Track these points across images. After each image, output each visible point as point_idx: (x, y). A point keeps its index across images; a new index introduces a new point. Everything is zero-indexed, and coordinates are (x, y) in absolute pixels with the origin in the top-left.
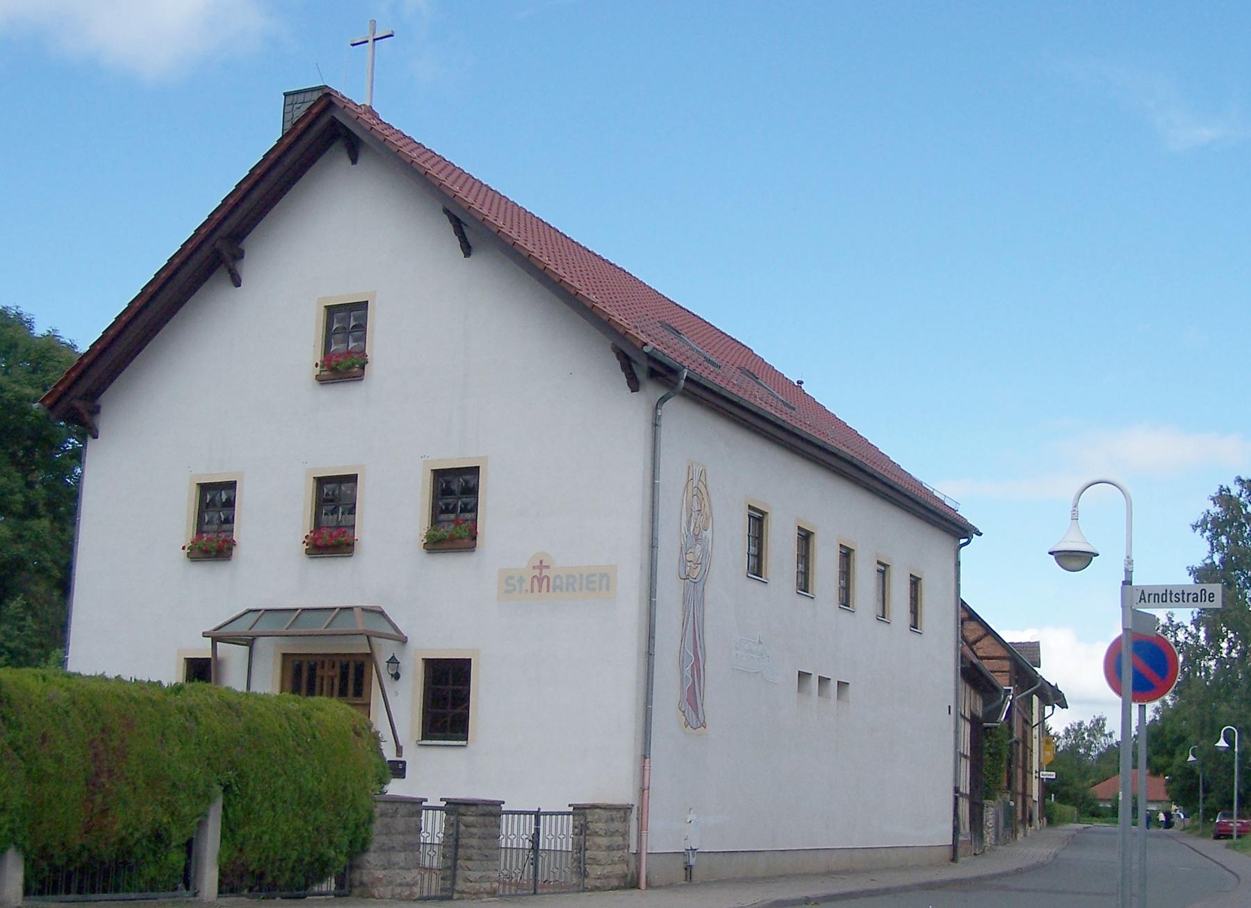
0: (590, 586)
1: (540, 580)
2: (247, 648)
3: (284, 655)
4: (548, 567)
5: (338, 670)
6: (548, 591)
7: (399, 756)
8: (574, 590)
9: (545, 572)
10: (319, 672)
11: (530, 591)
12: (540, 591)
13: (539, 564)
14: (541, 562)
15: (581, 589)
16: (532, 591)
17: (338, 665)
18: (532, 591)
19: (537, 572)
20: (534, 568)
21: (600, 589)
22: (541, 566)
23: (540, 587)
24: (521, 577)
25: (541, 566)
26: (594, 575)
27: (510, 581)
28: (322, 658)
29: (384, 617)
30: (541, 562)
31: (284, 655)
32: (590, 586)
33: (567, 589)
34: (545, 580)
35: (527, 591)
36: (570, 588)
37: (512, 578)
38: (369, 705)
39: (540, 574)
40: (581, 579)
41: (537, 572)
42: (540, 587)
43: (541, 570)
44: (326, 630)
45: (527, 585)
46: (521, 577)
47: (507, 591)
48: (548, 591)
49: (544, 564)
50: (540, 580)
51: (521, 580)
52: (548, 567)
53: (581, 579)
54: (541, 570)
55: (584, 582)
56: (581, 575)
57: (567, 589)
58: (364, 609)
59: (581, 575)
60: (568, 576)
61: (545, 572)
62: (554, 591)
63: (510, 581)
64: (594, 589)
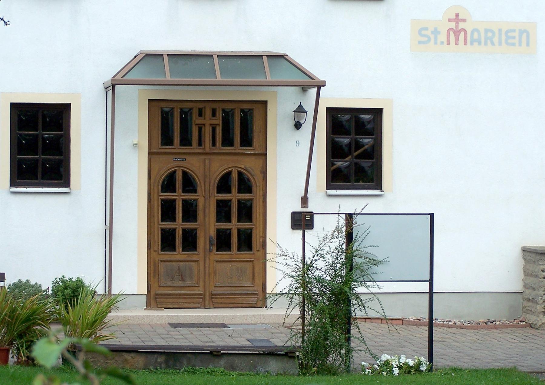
0: (510, 41)
1: (457, 33)
2: (116, 86)
3: (150, 101)
4: (464, 20)
5: (218, 121)
6: (465, 44)
7: (305, 207)
8: (493, 44)
9: (461, 25)
10: (196, 120)
11: (445, 43)
12: (456, 44)
13: (455, 17)
14: (457, 15)
15: (500, 44)
16: (448, 43)
17: (219, 114)
18: (448, 43)
19: (453, 25)
20: (450, 20)
21: (520, 45)
22: (457, 19)
23: (457, 39)
24: (436, 29)
25: (457, 19)
26: (514, 31)
27: (423, 32)
28: (201, 106)
29: (284, 58)
30: (457, 15)
31: (150, 101)
32: (510, 41)
33: (486, 44)
34: (462, 33)
35: (442, 43)
36: (489, 41)
37: (426, 29)
38: (264, 155)
39: (457, 27)
40: (500, 34)
41: (453, 25)
42: (457, 39)
43: (457, 23)
44: (122, 78)
45: (443, 37)
46: (436, 29)
47: (420, 42)
48: (465, 44)
49: (460, 17)
50: (457, 33)
51: (436, 32)
52: (464, 20)
53: (500, 34)
54: (457, 23)
55: (503, 38)
56: (500, 30)
57: (486, 44)
58: (171, 56)
59: (500, 30)
60: (487, 31)
61: (461, 25)
62: (472, 44)
63: (423, 32)
64: (514, 44)
